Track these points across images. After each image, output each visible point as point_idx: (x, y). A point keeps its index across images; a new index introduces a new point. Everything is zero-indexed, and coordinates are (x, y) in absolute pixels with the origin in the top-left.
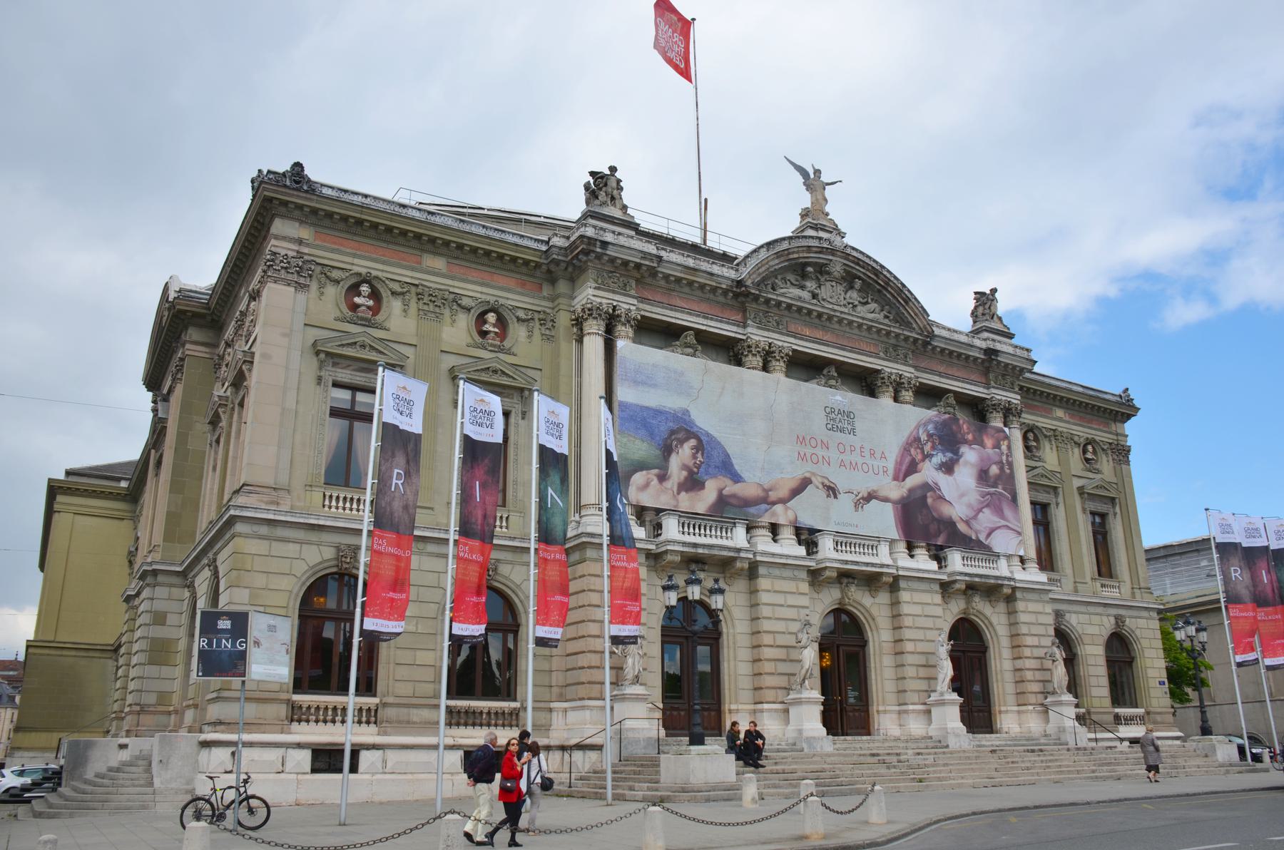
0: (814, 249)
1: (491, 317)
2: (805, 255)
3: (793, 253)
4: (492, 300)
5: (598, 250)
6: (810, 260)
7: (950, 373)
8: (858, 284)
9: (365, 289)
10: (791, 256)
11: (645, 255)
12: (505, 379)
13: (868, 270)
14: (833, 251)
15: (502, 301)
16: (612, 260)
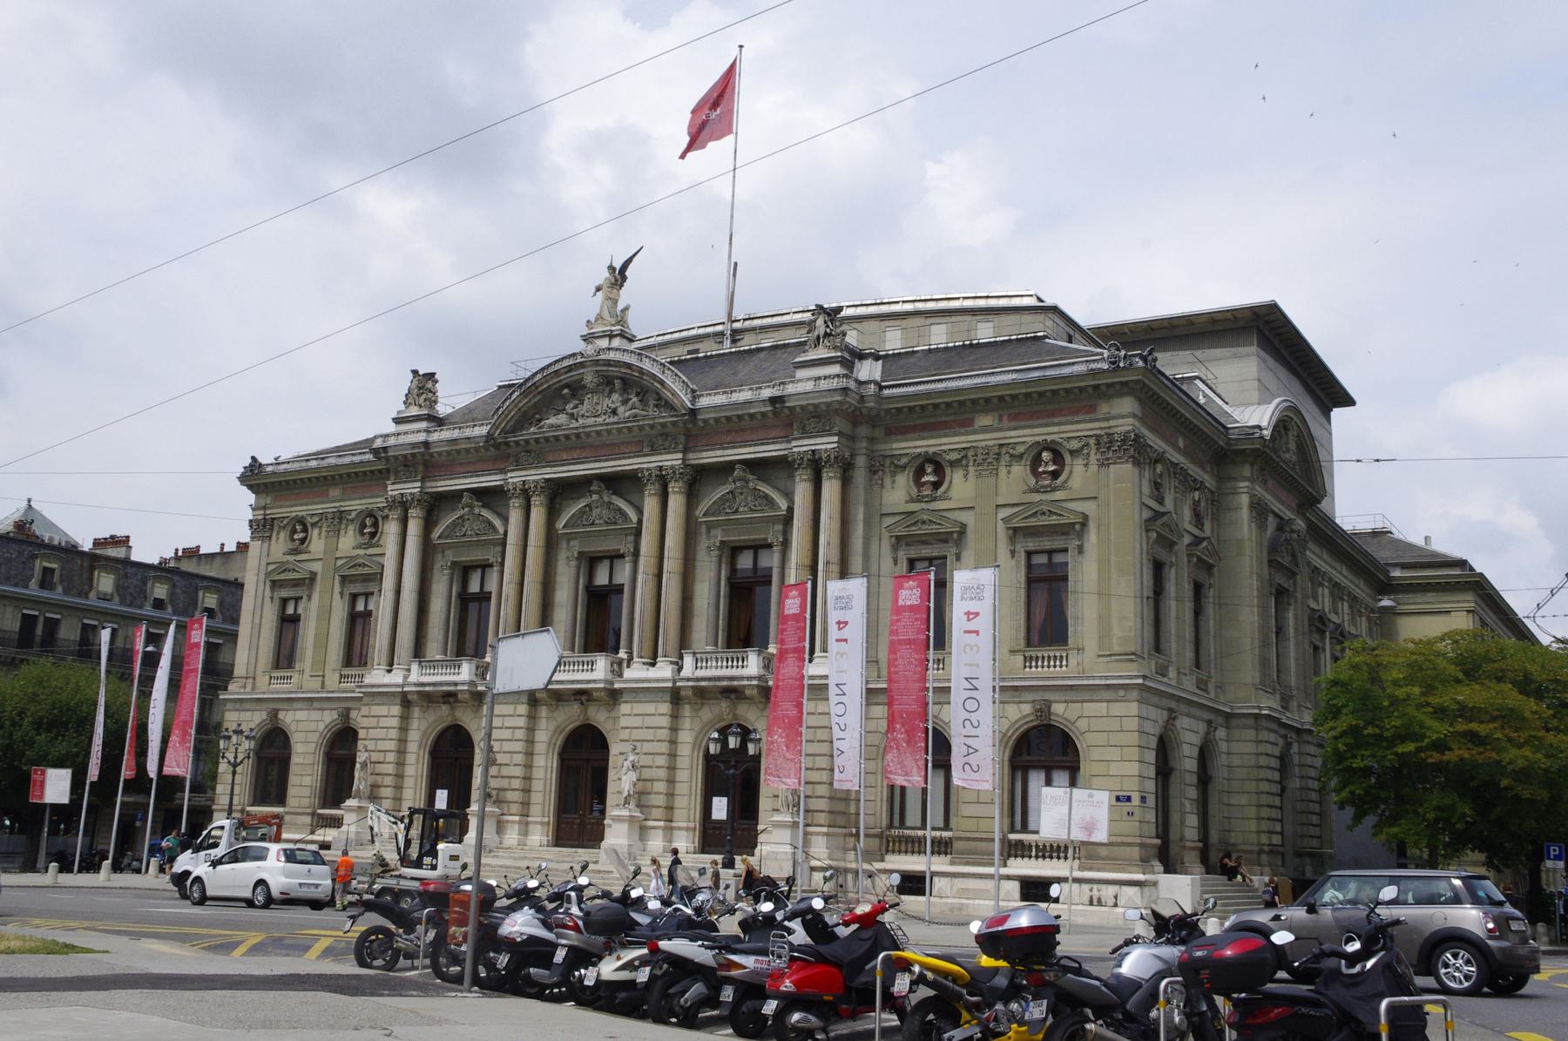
0: (562, 371)
1: (368, 521)
2: (556, 380)
3: (542, 384)
4: (364, 507)
5: (383, 455)
6: (565, 382)
7: (739, 439)
9: (299, 528)
10: (541, 389)
11: (414, 445)
13: (621, 367)
14: (582, 365)
15: (370, 507)
16: (396, 457)
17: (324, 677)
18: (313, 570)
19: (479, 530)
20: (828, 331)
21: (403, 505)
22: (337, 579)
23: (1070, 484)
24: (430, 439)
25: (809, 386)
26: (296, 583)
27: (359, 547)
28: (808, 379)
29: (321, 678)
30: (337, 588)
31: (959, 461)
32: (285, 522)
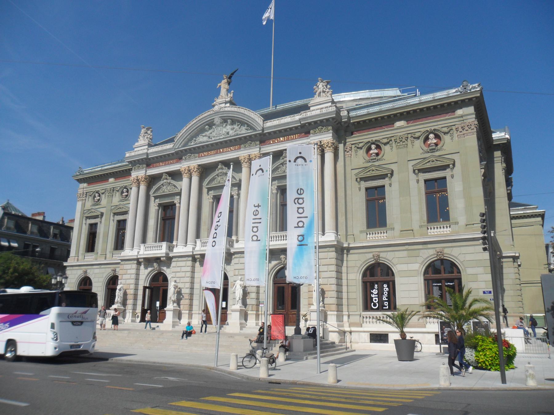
4: (122, 185)
8: (229, 121)
9: (97, 195)
12: (378, 172)
17: (106, 255)
18: (102, 211)
19: (170, 189)
20: (324, 90)
21: (138, 181)
22: (112, 214)
23: (444, 147)
24: (149, 152)
25: (318, 112)
26: (96, 217)
27: (121, 201)
28: (317, 109)
29: (105, 255)
30: (112, 218)
31: (388, 143)
32: (91, 194)
